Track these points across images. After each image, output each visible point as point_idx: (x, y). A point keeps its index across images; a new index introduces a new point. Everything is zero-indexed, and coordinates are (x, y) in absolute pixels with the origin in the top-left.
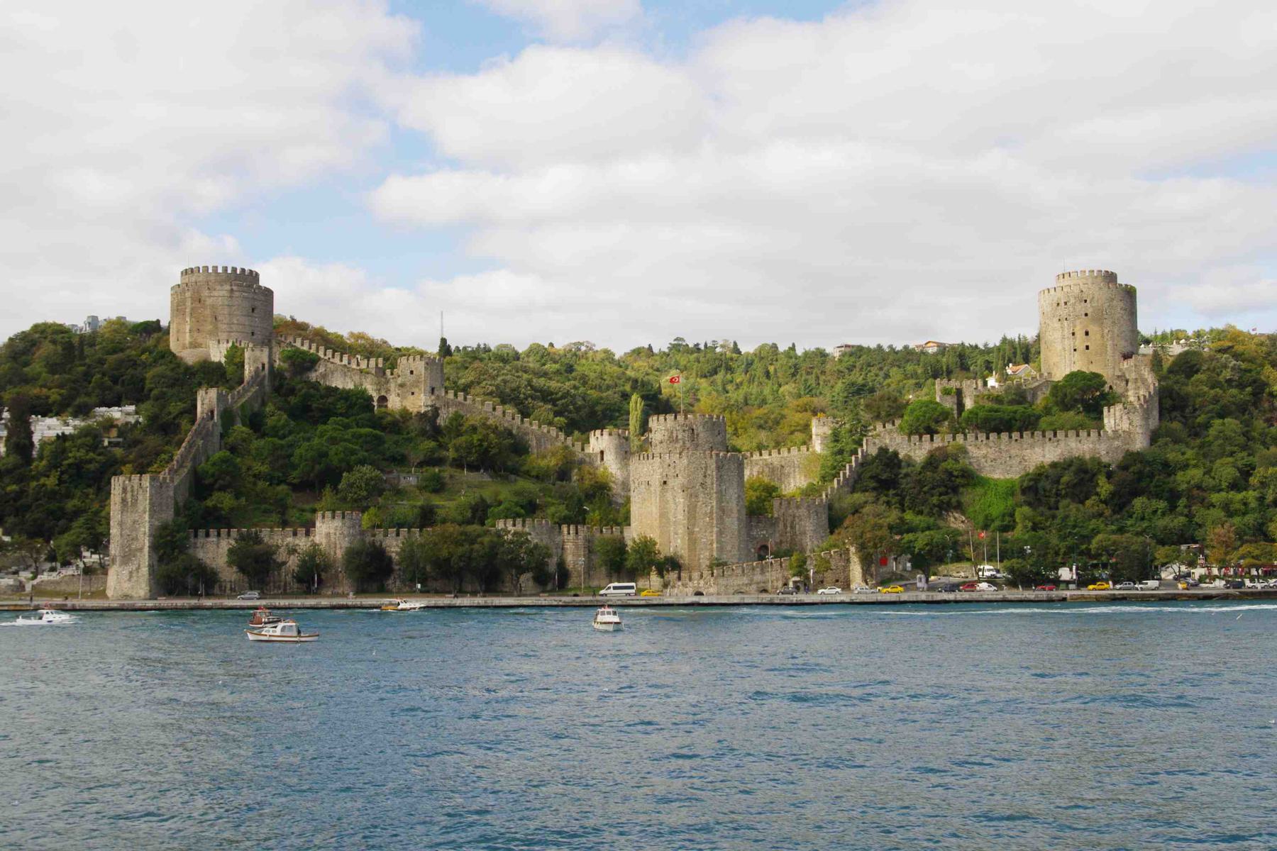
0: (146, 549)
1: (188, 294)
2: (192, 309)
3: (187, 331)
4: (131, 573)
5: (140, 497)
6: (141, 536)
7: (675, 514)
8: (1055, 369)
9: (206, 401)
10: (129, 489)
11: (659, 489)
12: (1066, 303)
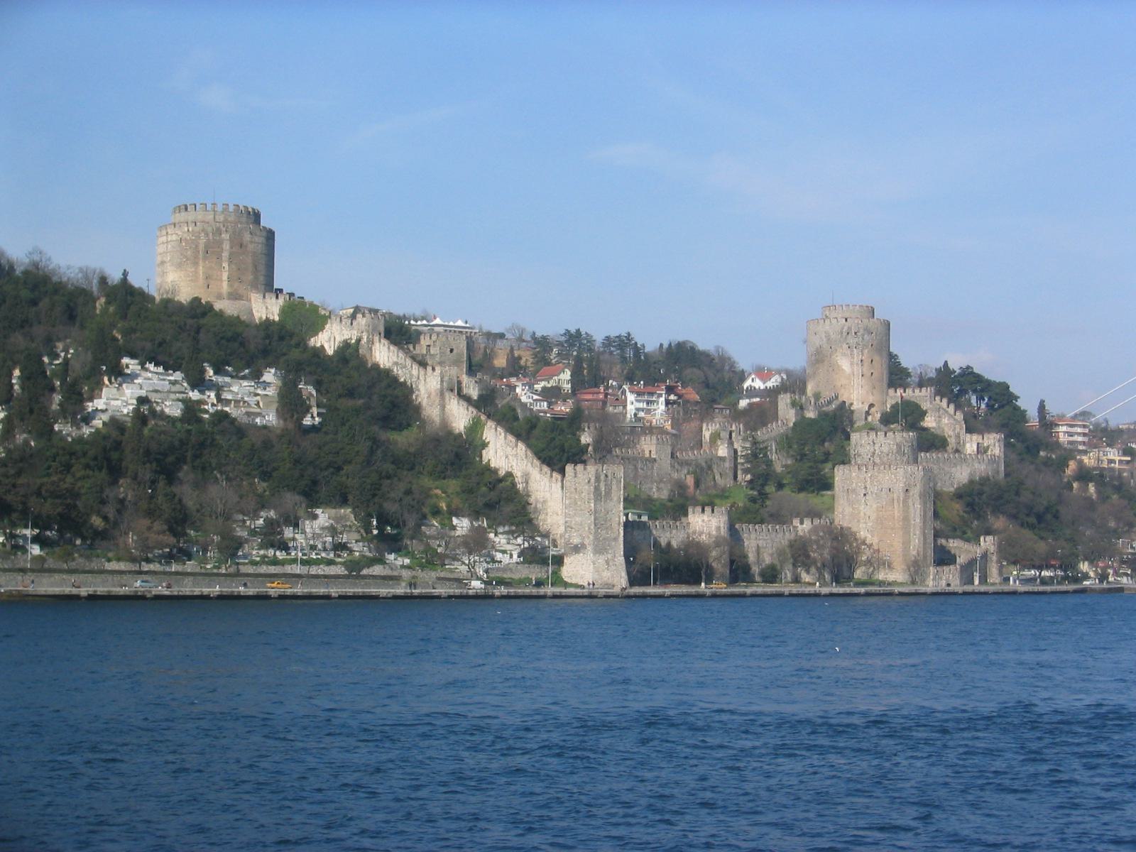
0: (621, 538)
1: (226, 236)
2: (231, 254)
3: (225, 276)
4: (607, 562)
5: (614, 487)
6: (615, 525)
7: (914, 517)
8: (843, 390)
9: (446, 378)
10: (602, 477)
11: (902, 496)
12: (855, 333)
